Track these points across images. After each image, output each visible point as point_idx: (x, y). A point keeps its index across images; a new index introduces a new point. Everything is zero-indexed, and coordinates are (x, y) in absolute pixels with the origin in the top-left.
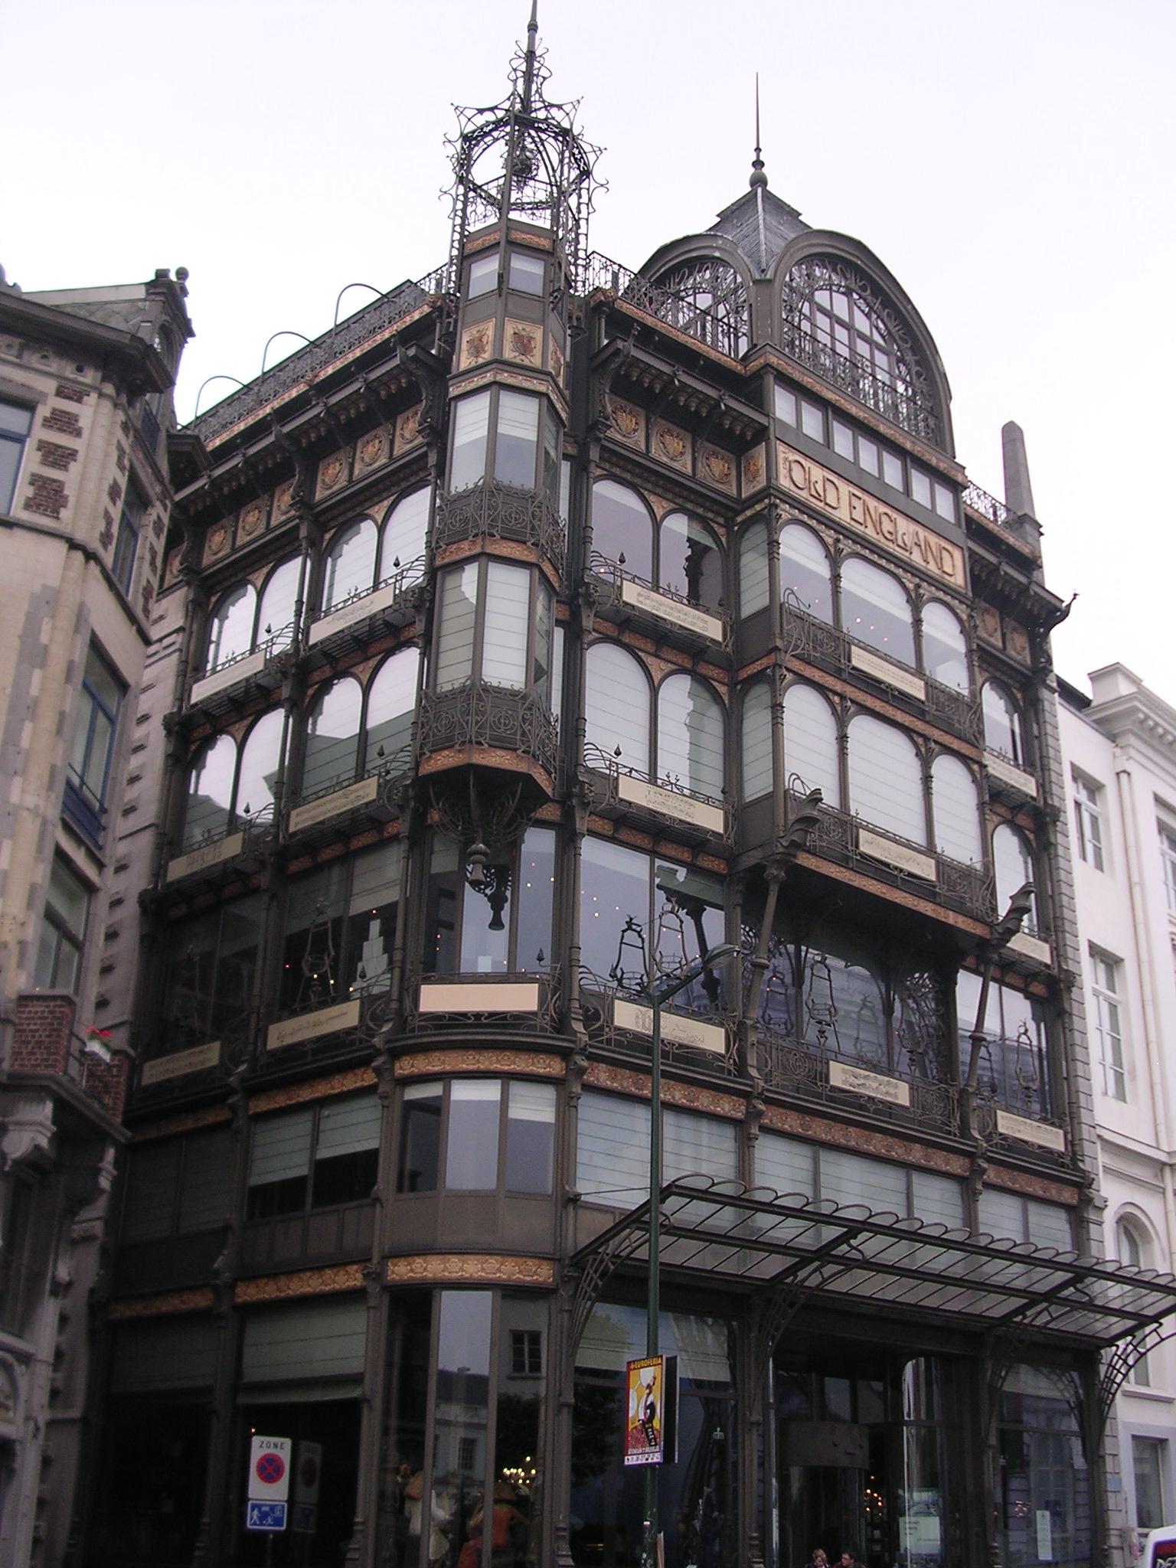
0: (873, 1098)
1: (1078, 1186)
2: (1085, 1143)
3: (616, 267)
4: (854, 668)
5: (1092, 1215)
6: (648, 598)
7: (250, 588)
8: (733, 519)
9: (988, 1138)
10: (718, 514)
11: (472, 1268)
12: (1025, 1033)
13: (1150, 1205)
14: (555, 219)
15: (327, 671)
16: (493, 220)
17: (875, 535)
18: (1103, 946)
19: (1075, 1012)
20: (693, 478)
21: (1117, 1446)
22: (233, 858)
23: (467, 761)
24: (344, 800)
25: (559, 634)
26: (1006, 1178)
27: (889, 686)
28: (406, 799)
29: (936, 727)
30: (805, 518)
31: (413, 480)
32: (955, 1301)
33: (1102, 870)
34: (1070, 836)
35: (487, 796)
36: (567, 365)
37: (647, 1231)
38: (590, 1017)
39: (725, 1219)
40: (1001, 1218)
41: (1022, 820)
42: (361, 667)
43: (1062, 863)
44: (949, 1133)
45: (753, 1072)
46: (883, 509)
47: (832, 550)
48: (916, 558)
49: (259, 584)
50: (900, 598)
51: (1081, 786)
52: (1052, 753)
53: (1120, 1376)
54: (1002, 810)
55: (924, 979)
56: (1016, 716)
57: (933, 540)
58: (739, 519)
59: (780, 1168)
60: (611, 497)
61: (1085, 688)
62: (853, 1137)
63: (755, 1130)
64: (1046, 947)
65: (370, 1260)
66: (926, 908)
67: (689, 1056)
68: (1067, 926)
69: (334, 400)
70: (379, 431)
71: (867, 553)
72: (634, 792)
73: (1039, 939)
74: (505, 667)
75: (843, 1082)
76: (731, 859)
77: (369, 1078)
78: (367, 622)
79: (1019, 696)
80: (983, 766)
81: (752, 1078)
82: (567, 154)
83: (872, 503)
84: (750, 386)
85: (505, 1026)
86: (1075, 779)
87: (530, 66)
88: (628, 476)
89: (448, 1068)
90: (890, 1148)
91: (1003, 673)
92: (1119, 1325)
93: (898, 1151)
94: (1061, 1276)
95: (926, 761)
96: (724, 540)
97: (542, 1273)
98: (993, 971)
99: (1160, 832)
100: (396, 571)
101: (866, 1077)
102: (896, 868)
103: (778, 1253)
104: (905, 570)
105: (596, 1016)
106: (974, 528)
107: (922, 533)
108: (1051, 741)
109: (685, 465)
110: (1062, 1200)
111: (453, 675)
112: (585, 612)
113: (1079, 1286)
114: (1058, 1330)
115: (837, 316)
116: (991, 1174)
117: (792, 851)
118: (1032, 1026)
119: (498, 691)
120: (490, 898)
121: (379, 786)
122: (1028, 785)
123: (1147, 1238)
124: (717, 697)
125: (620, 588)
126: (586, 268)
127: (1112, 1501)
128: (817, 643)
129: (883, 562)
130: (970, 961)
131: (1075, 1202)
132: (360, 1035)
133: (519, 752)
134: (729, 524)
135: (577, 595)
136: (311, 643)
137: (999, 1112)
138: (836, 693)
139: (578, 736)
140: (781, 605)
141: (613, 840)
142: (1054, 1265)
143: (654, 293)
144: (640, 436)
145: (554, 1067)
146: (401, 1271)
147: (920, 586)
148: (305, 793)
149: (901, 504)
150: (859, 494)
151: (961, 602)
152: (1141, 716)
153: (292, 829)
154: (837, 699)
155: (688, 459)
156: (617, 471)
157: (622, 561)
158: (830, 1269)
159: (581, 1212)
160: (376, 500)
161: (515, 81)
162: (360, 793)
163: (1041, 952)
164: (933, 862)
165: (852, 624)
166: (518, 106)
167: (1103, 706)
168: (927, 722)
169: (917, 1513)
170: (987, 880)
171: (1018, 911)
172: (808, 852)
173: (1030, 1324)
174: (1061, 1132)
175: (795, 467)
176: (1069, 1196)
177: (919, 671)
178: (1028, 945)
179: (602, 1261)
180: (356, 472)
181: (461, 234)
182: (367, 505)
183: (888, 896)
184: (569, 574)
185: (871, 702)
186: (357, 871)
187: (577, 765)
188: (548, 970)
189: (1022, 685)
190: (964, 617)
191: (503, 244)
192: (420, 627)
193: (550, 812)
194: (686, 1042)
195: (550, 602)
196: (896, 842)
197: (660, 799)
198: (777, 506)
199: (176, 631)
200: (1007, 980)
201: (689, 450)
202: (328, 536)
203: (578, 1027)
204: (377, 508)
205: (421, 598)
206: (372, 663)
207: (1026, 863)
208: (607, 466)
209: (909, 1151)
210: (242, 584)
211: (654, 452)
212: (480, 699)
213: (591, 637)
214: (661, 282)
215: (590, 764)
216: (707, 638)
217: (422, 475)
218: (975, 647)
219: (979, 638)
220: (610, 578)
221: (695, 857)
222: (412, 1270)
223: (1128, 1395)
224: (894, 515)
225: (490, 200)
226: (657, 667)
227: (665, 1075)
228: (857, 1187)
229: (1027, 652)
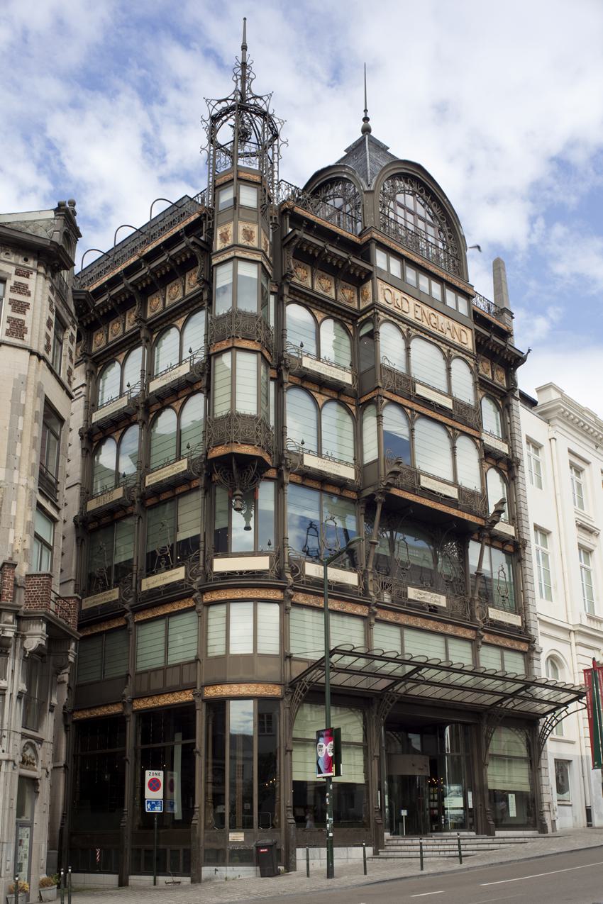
1: (528, 642)
2: (532, 622)
3: (293, 188)
4: (417, 395)
5: (535, 656)
6: (315, 364)
7: (117, 363)
8: (356, 320)
9: (484, 621)
10: (348, 318)
11: (243, 690)
12: (502, 570)
13: (564, 651)
14: (261, 163)
15: (159, 406)
16: (229, 166)
17: (427, 326)
18: (542, 526)
19: (527, 559)
20: (336, 301)
21: (547, 764)
22: (119, 499)
23: (230, 451)
24: (171, 470)
25: (272, 385)
26: (493, 639)
27: (435, 403)
28: (201, 469)
29: (458, 421)
30: (392, 319)
31: (196, 307)
32: (470, 698)
33: (541, 488)
34: (526, 474)
35: (238, 467)
36: (271, 243)
37: (324, 670)
38: (294, 571)
39: (361, 663)
40: (490, 659)
41: (502, 465)
42: (176, 403)
43: (521, 486)
44: (466, 619)
45: (372, 594)
46: (431, 311)
48: (448, 336)
49: (121, 360)
50: (439, 357)
51: (531, 446)
52: (516, 431)
53: (548, 732)
54: (491, 461)
55: (452, 547)
56: (498, 413)
57: (457, 326)
58: (359, 321)
59: (387, 640)
60: (296, 314)
61: (533, 395)
62: (420, 623)
63: (373, 621)
64: (513, 528)
65: (196, 688)
66: (454, 512)
67: (340, 590)
68: (523, 517)
69: (153, 265)
70: (177, 281)
71: (423, 335)
72: (311, 462)
73: (510, 524)
74: (247, 404)
76: (359, 492)
77: (191, 603)
78: (177, 381)
79: (500, 403)
80: (481, 441)
81: (371, 597)
82: (266, 126)
83: (426, 309)
84: (363, 251)
85: (254, 577)
86: (528, 443)
88: (303, 301)
89: (228, 597)
90: (437, 627)
91: (493, 392)
92: (548, 708)
93: (441, 628)
94: (518, 686)
95: (453, 440)
96: (352, 331)
97: (276, 691)
98: (486, 541)
99: (571, 468)
100: (190, 355)
101: (425, 594)
102: (439, 493)
103: (385, 678)
104: (443, 343)
105: (297, 571)
106: (478, 318)
107: (452, 323)
108: (516, 425)
109: (331, 294)
110: (520, 649)
111: (221, 409)
112: (284, 374)
113: (528, 690)
114: (518, 710)
115: (408, 210)
116: (486, 638)
117: (388, 488)
118: (506, 566)
119: (244, 417)
120: (244, 516)
121: (188, 462)
122: (504, 448)
123: (562, 667)
124: (350, 412)
125: (301, 359)
126: (279, 189)
127: (544, 789)
128: (398, 383)
129: (431, 339)
130: (476, 536)
131: (527, 650)
132: (185, 583)
133: (256, 446)
134: (354, 322)
135: (279, 365)
136: (150, 392)
137: (490, 609)
138: (408, 408)
139: (283, 435)
140: (381, 365)
141: (302, 485)
142: (514, 680)
143: (314, 201)
144: (309, 280)
145: (278, 595)
146: (211, 692)
147: (449, 351)
148: (152, 467)
150: (419, 304)
151: (471, 357)
152: (563, 410)
153: (147, 485)
155: (333, 290)
156: (297, 299)
157: (302, 346)
158: (409, 685)
159: (293, 663)
160: (178, 317)
161: (236, 82)
162: (180, 466)
163: (510, 531)
164: (456, 490)
165: (416, 373)
166: (239, 97)
167: (543, 406)
168: (454, 420)
169: (451, 796)
170: (484, 497)
171: (498, 512)
172: (396, 487)
173: (505, 708)
174: (520, 617)
175: (387, 292)
176: (524, 647)
177: (449, 394)
178: (503, 527)
179: (303, 684)
180: (167, 303)
181: (214, 175)
182: (173, 320)
183: (434, 507)
184: (276, 354)
186: (179, 505)
187: (283, 450)
188: (273, 550)
189: (501, 397)
190: (472, 365)
191: (235, 180)
192: (204, 383)
193: (272, 473)
194: (339, 581)
195: (267, 369)
196: (438, 480)
197: (324, 465)
198: (378, 314)
199: (82, 386)
200: (493, 544)
201: (333, 285)
202: (155, 336)
203: (288, 575)
204: (178, 321)
205: (203, 369)
206: (181, 401)
207: (503, 487)
208: (293, 296)
209: (446, 629)
210: (113, 361)
211: (317, 288)
212: (235, 420)
214: (315, 193)
215: (290, 449)
216: (344, 383)
217: (200, 304)
218: (477, 380)
219: (480, 375)
220: (296, 355)
221: (341, 491)
222: (216, 692)
223: (552, 740)
224: (437, 314)
225: (228, 153)
226: (321, 399)
227: (330, 597)
228: (424, 647)
229: (504, 380)
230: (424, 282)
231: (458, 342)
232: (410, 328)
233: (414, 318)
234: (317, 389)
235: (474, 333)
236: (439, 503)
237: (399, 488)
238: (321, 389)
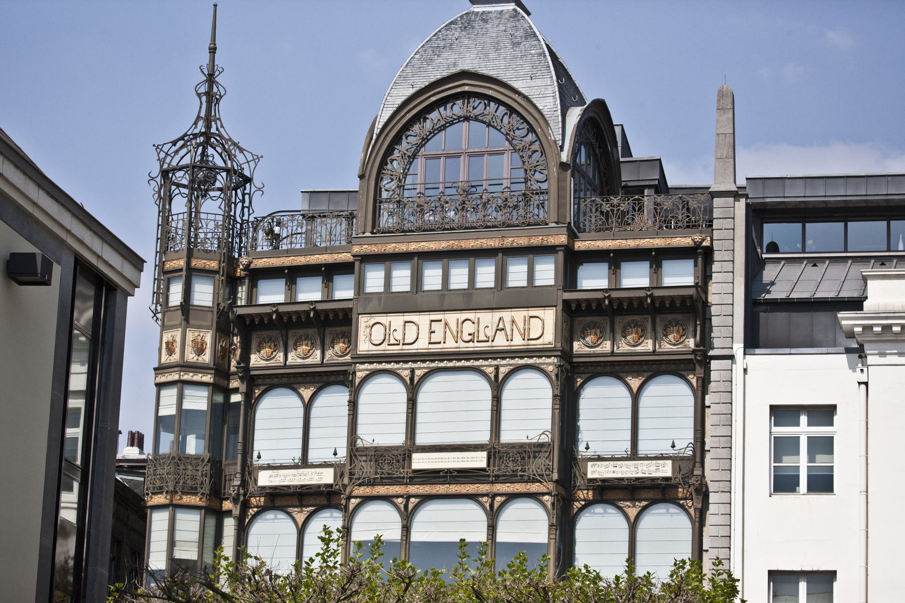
27: (449, 471)
47: (408, 379)
48: (501, 342)
54: (651, 495)
57: (519, 315)
83: (452, 318)
87: (211, 87)
129: (463, 363)
154: (400, 500)
168: (492, 483)
190: (551, 368)
213: (252, 512)
231: (521, 342)
233: (426, 345)
234: (295, 501)
235: (560, 307)
238: (301, 500)
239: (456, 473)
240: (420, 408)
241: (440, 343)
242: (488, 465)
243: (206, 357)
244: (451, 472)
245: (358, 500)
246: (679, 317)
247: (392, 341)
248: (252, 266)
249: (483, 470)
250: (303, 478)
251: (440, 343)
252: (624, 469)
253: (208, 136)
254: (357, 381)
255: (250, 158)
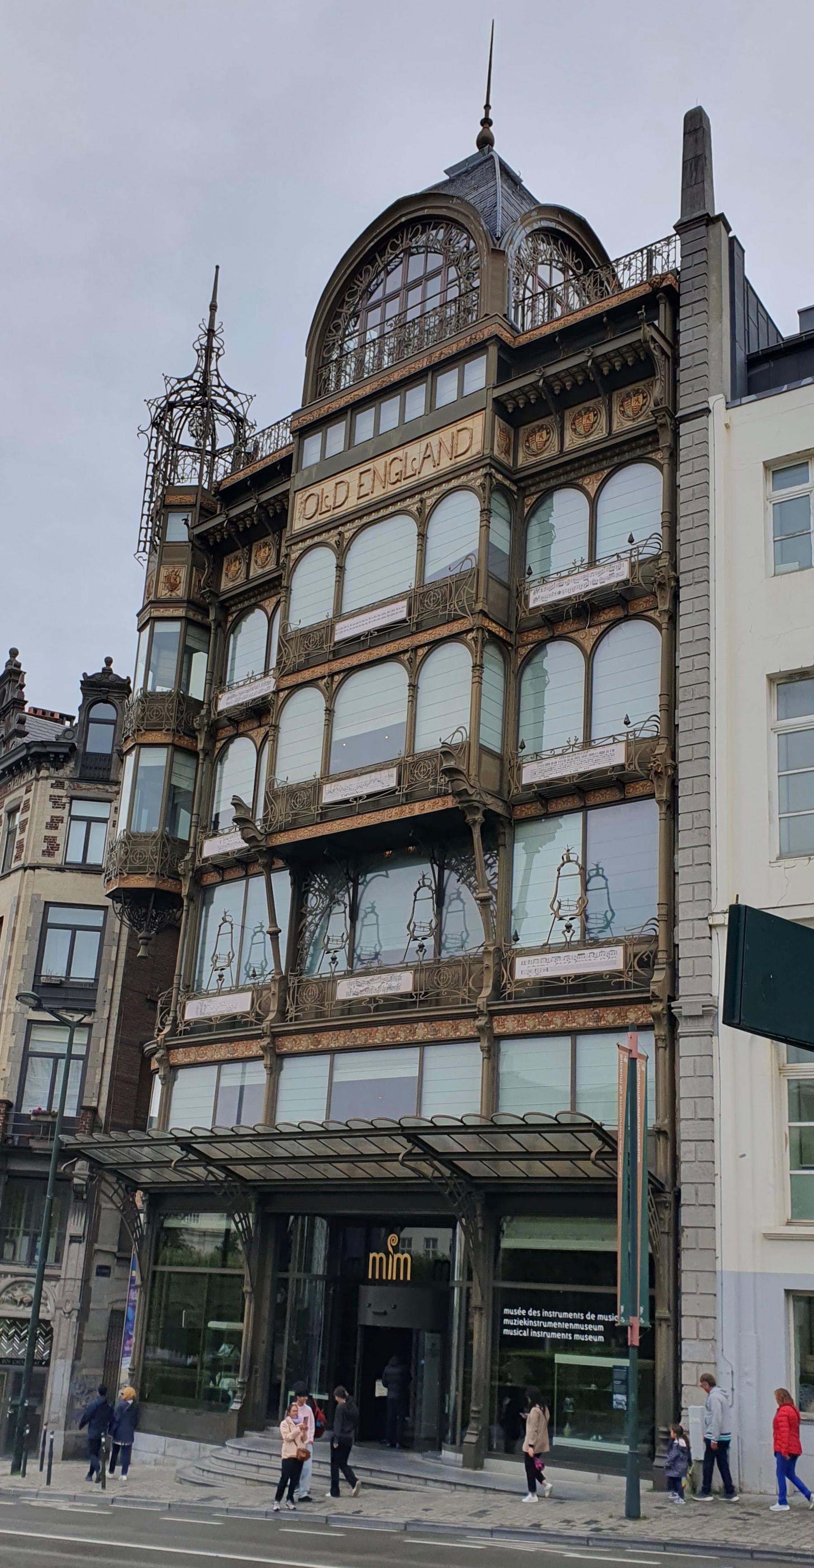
0: (373, 999)
4: (335, 644)
27: (369, 633)
54: (610, 615)
71: (374, 516)
75: (347, 994)
83: (379, 464)
87: (209, 341)
102: (355, 799)
129: (391, 509)
149: (438, 420)
156: (246, 603)
168: (413, 634)
172: (281, 831)
185: (354, 661)
230: (390, 409)
232: (341, 529)
236: (359, 814)
237: (285, 831)
239: (376, 634)
240: (348, 576)
241: (367, 495)
242: (409, 613)
243: (181, 592)
244: (371, 634)
245: (287, 692)
246: (640, 385)
247: (324, 509)
248: (222, 488)
249: (404, 621)
250: (254, 691)
251: (367, 495)
252: (572, 585)
253: (204, 388)
254: (291, 564)
255: (243, 399)
